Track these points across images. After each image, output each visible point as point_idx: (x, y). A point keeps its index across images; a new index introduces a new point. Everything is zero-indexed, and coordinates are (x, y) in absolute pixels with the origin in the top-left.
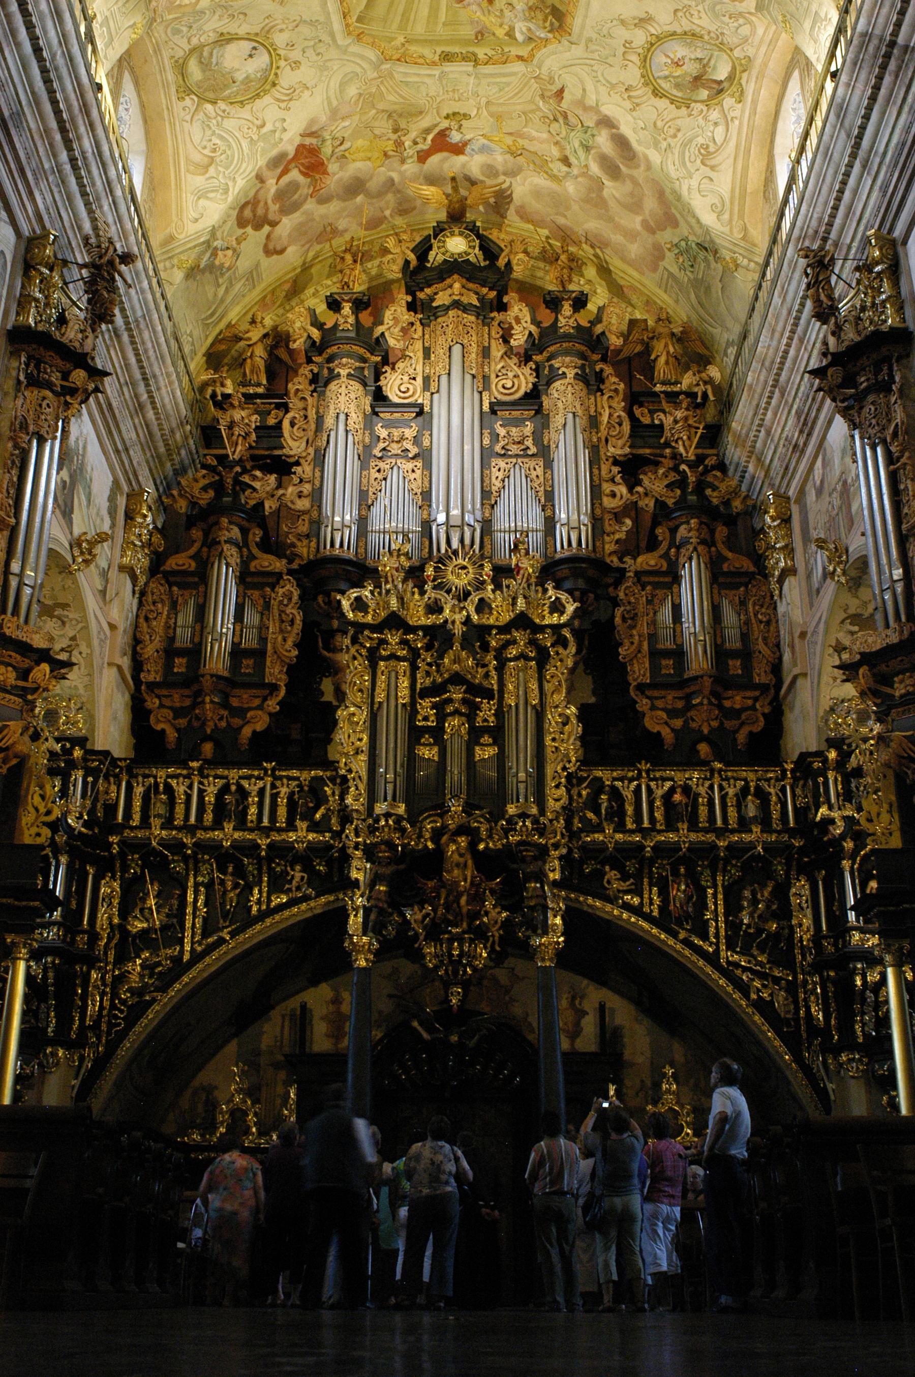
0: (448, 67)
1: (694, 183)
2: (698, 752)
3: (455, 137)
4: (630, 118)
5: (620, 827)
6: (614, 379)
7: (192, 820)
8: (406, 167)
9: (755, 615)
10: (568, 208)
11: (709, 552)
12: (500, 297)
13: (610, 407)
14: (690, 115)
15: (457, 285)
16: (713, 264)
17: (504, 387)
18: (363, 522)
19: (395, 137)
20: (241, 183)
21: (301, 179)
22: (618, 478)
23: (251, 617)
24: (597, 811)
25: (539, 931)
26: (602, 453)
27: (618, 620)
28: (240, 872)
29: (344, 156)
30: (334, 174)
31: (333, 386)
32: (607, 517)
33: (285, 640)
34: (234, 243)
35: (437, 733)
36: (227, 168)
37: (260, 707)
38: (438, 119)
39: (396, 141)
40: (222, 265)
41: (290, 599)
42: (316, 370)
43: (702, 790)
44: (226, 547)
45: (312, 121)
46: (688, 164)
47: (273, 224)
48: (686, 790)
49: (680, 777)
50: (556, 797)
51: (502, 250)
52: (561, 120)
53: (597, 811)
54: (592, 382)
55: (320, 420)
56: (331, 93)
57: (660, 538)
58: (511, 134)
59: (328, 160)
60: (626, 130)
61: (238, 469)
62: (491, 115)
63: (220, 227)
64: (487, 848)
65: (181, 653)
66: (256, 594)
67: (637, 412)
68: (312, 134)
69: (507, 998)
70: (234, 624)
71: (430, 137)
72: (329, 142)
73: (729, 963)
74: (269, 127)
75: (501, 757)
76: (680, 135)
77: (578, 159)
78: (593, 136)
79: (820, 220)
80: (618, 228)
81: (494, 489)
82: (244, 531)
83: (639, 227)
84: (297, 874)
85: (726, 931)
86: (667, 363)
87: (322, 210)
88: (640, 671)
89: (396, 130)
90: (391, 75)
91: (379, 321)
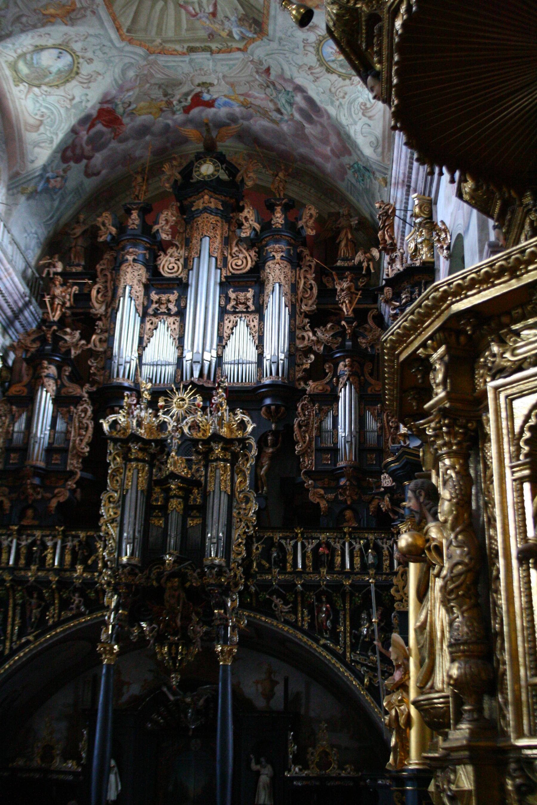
0: (194, 56)
1: (358, 127)
2: (344, 516)
3: (206, 97)
4: (313, 87)
5: (283, 570)
6: (308, 258)
7: (11, 563)
8: (176, 117)
9: (388, 423)
10: (286, 139)
11: (360, 380)
12: (238, 202)
13: (305, 277)
14: (352, 84)
15: (206, 197)
16: (374, 181)
17: (236, 265)
18: (140, 357)
19: (165, 99)
20: (61, 136)
21: (104, 129)
22: (308, 327)
23: (60, 426)
24: (269, 561)
25: (221, 642)
26: (298, 310)
28: (41, 597)
29: (133, 113)
30: (127, 124)
31: (123, 267)
32: (298, 354)
33: (81, 440)
34: (62, 173)
35: (164, 508)
36: (51, 127)
37: (64, 486)
38: (193, 87)
39: (167, 102)
40: (54, 188)
41: (86, 414)
42: (115, 255)
43: (338, 546)
44: (46, 380)
45: (106, 95)
46: (354, 116)
47: (89, 158)
48: (328, 545)
49: (323, 537)
50: (239, 552)
51: (238, 171)
52: (271, 87)
54: (294, 261)
56: (117, 76)
57: (327, 371)
58: (242, 95)
60: (312, 93)
61: (55, 328)
62: (227, 83)
63: (49, 165)
64: (191, 585)
65: (16, 450)
66: (65, 409)
67: (325, 280)
68: (108, 102)
70: (50, 430)
71: (189, 98)
72: (120, 106)
73: (352, 661)
74: (77, 100)
76: (347, 97)
77: (286, 110)
78: (293, 97)
79: (404, 174)
80: (318, 153)
81: (225, 335)
82: (59, 369)
83: (329, 153)
84: (76, 599)
85: (351, 641)
86: (346, 245)
87: (122, 147)
88: (308, 462)
89: (166, 95)
90: (155, 62)
91: (156, 222)
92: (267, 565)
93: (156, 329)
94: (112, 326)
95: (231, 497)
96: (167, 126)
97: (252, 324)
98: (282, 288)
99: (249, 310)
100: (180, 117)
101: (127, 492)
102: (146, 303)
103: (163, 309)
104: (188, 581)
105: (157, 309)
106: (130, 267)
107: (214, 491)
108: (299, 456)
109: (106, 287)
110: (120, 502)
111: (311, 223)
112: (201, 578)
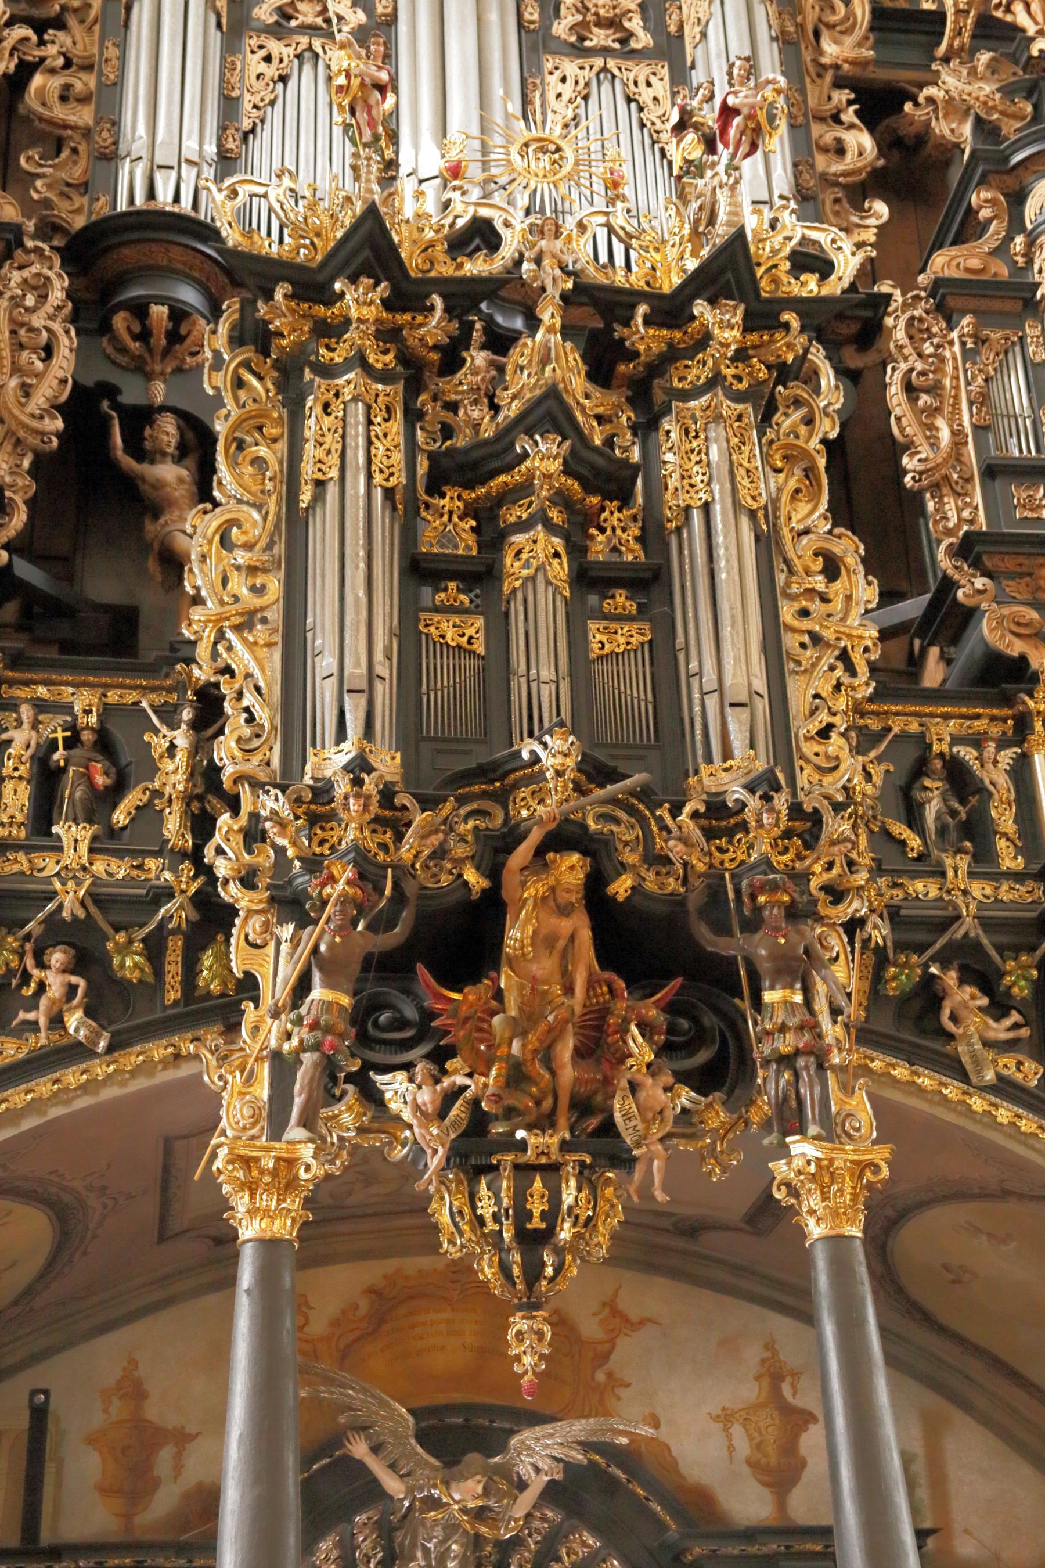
22: (849, 115)
25: (813, 1130)
26: (807, 57)
27: (895, 393)
35: (481, 575)
41: (43, 298)
53: (913, 817)
57: (985, 213)
69: (600, 1376)
75: (664, 657)
92: (915, 842)
93: (283, 79)
95: (768, 544)
97: (646, 95)
99: (634, 45)
101: (319, 497)
104: (624, 867)
107: (706, 507)
108: (920, 493)
110: (280, 549)
112: (710, 834)
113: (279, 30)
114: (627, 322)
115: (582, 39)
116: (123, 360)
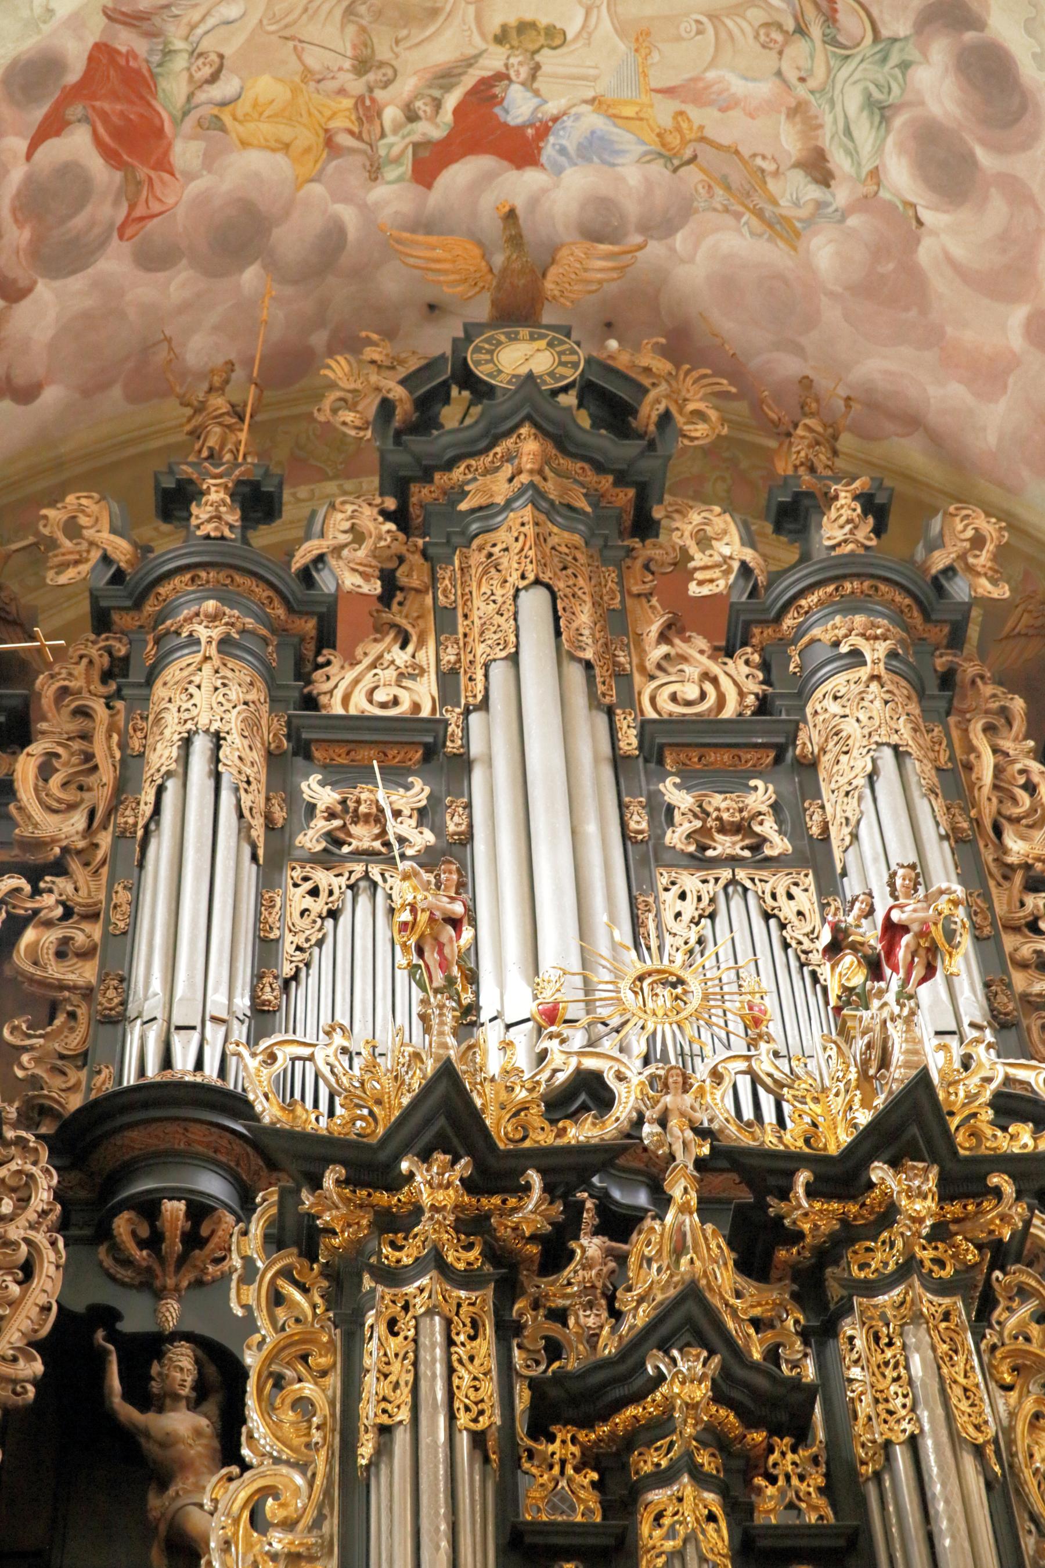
3: (518, 107)
8: (379, 193)
13: (996, 751)
17: (674, 698)
19: (357, 86)
21: (96, 164)
26: (988, 856)
30: (190, 177)
38: (479, 43)
39: (360, 100)
41: (23, 1202)
55: (131, 764)
58: (668, 92)
59: (177, 123)
62: (621, 32)
71: (452, 101)
72: (180, 62)
77: (852, 153)
78: (905, 66)
83: (1016, 341)
89: (363, 65)
93: (333, 915)
94: (122, 896)
96: (334, 238)
97: (787, 910)
98: (913, 766)
99: (768, 851)
100: (392, 196)
101: (383, 1450)
102: (279, 815)
103: (363, 836)
105: (335, 840)
106: (207, 668)
107: (913, 1443)
109: (89, 757)
110: (331, 1526)
111: (982, 559)
113: (326, 859)
114: (784, 1193)
115: (704, 848)
116: (124, 1274)
